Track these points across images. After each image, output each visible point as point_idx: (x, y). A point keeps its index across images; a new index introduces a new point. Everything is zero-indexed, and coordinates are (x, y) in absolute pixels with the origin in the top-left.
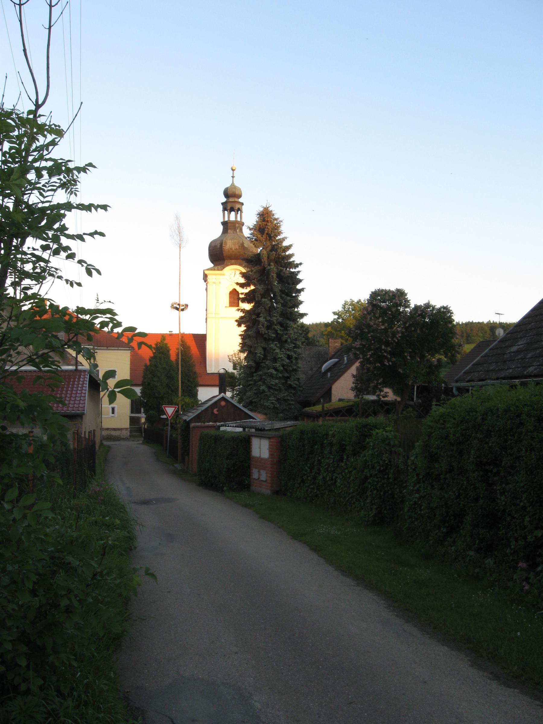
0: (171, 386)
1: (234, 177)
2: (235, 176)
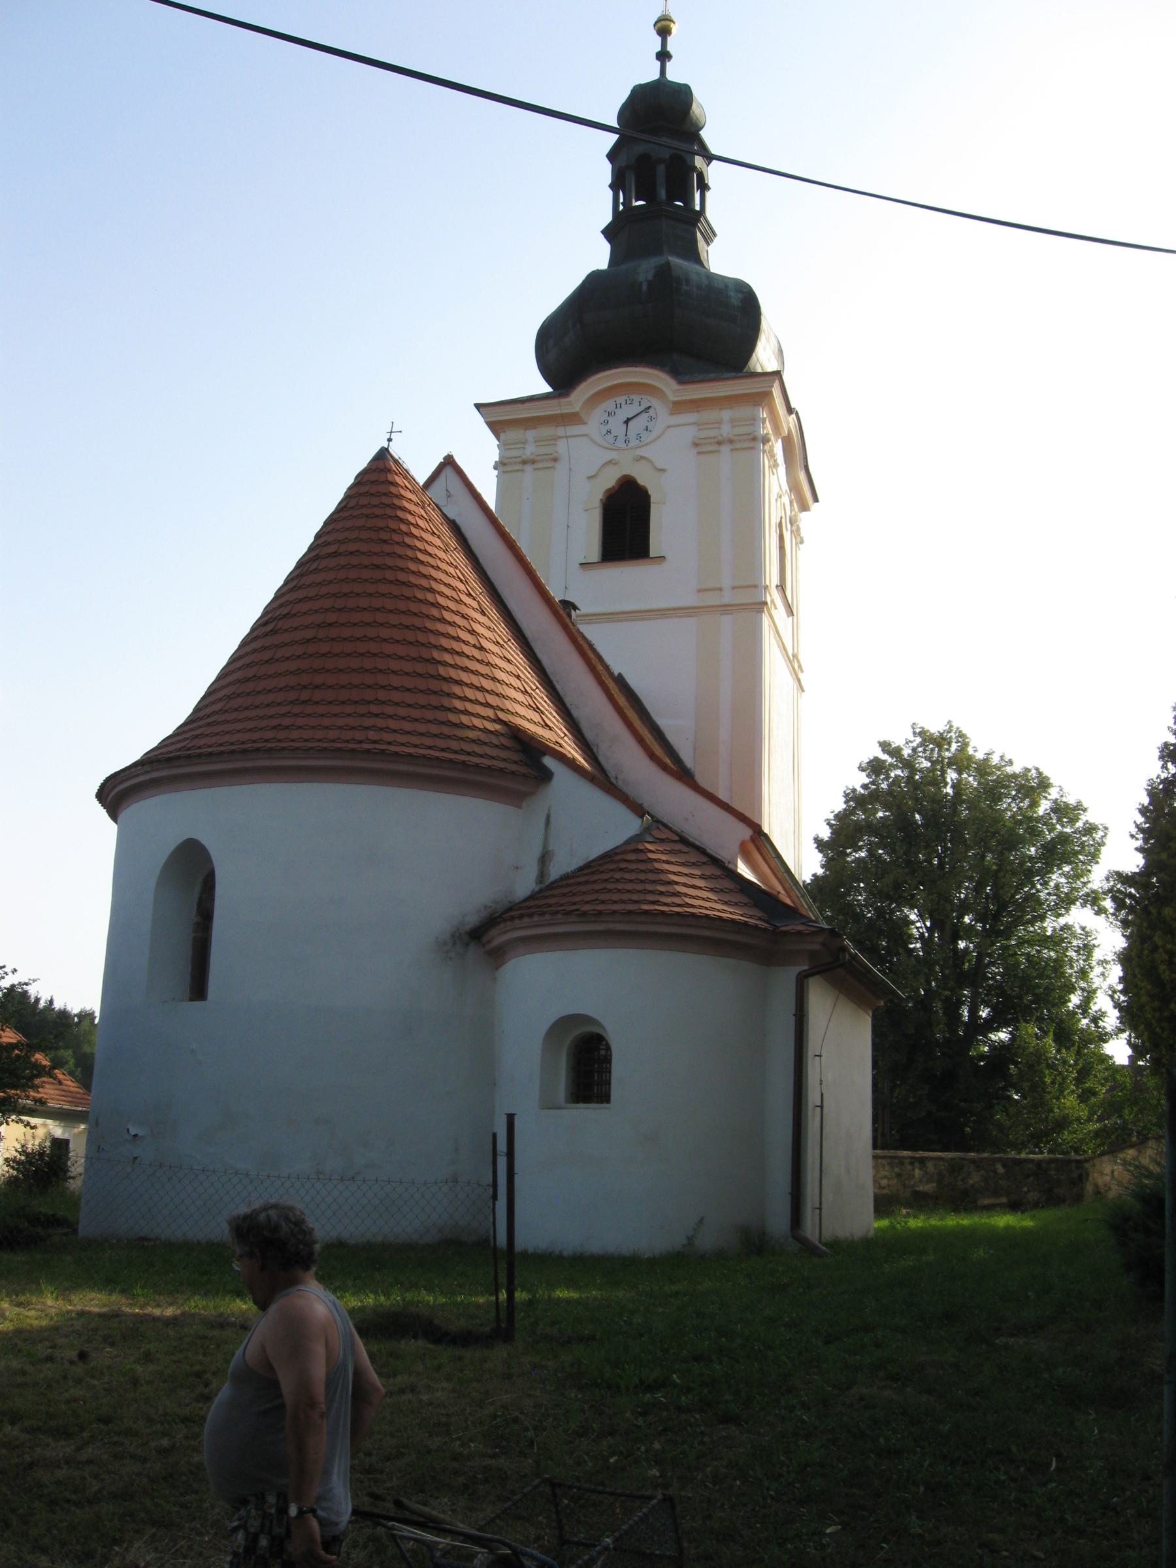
2: (669, 48)
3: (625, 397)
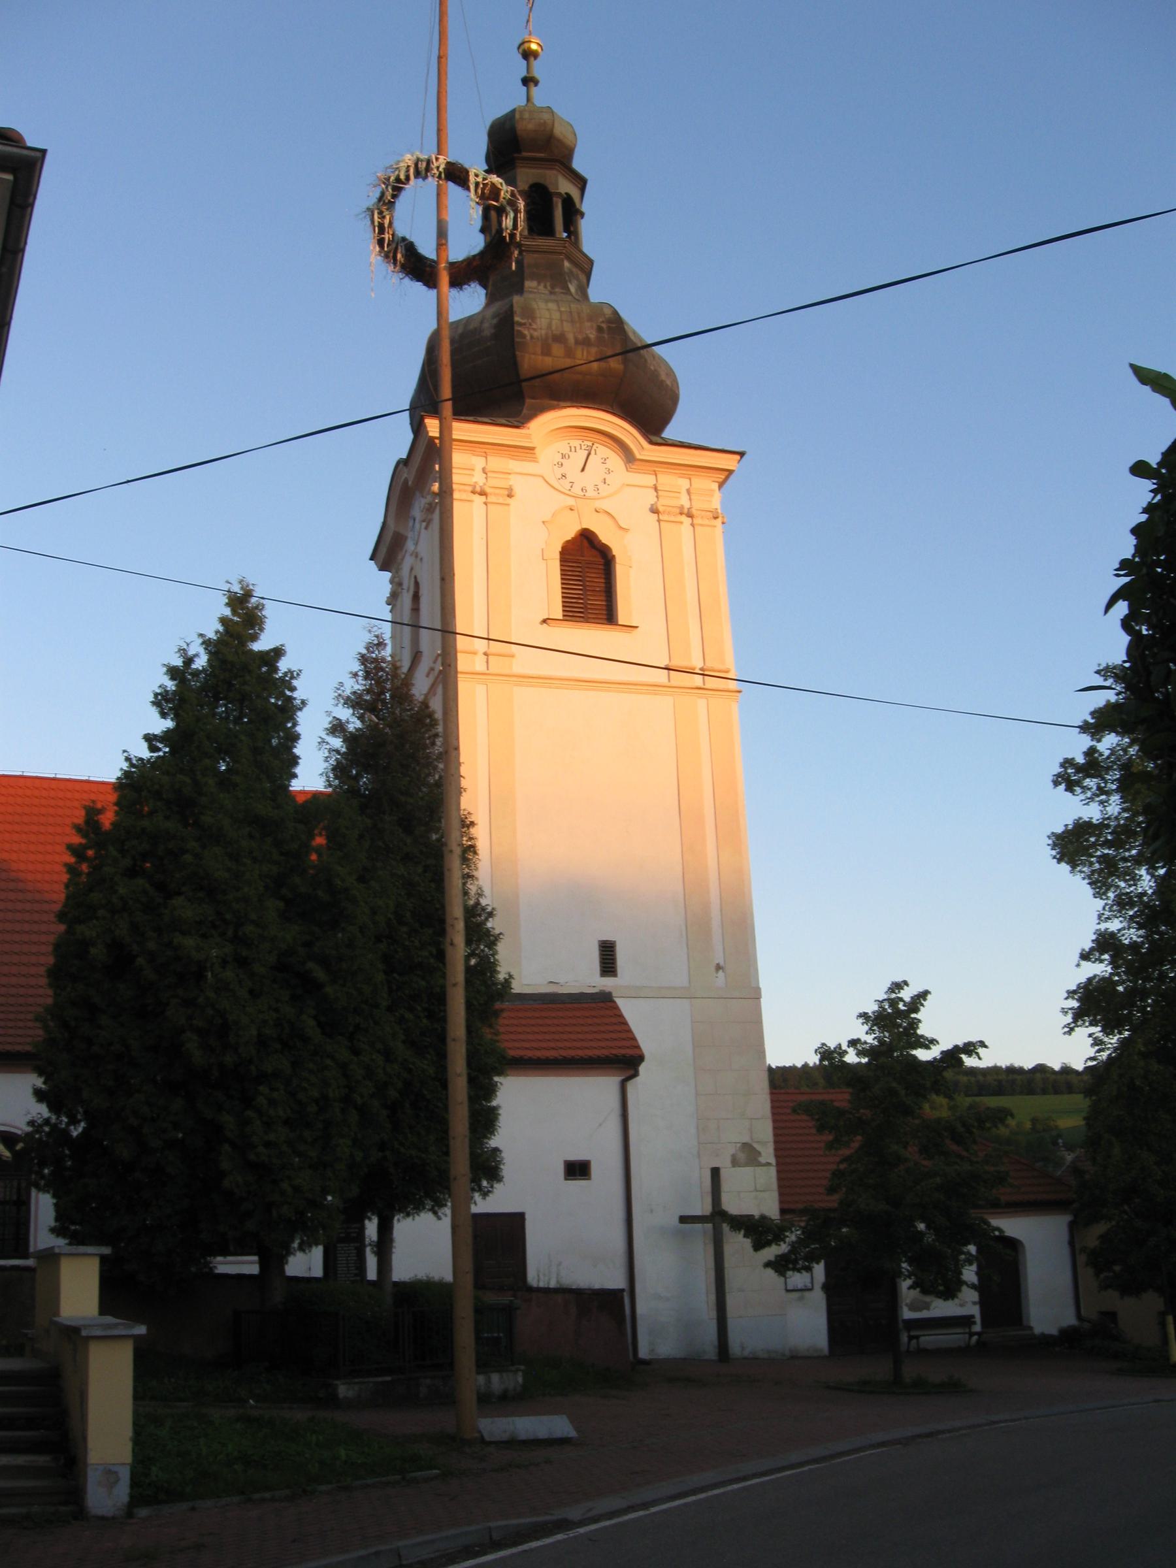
0: (320, 974)
1: (536, 83)
3: (580, 442)
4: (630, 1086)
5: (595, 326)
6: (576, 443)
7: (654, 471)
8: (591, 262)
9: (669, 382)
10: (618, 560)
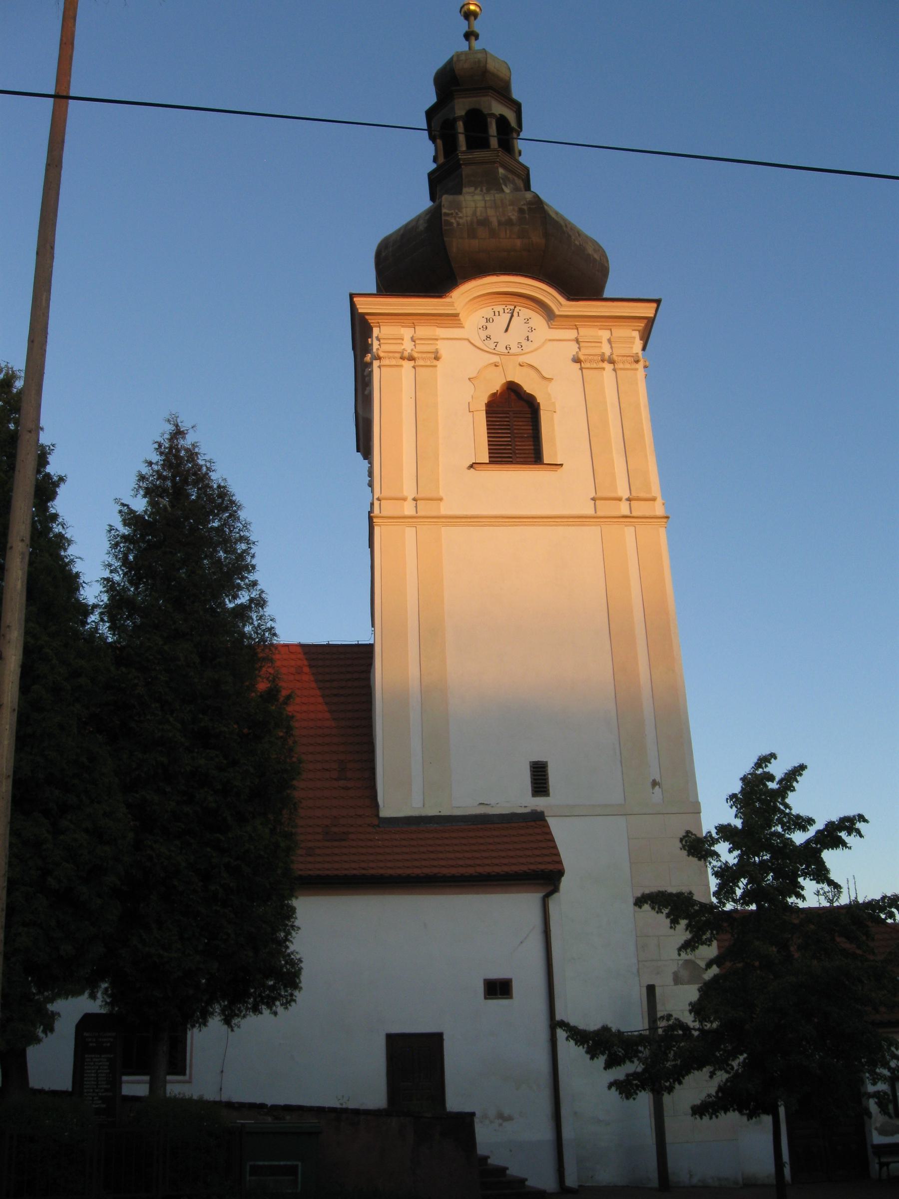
3: (504, 307)
4: (554, 904)
5: (516, 208)
6: (499, 308)
7: (576, 325)
8: (527, 170)
9: (596, 256)
10: (542, 407)
